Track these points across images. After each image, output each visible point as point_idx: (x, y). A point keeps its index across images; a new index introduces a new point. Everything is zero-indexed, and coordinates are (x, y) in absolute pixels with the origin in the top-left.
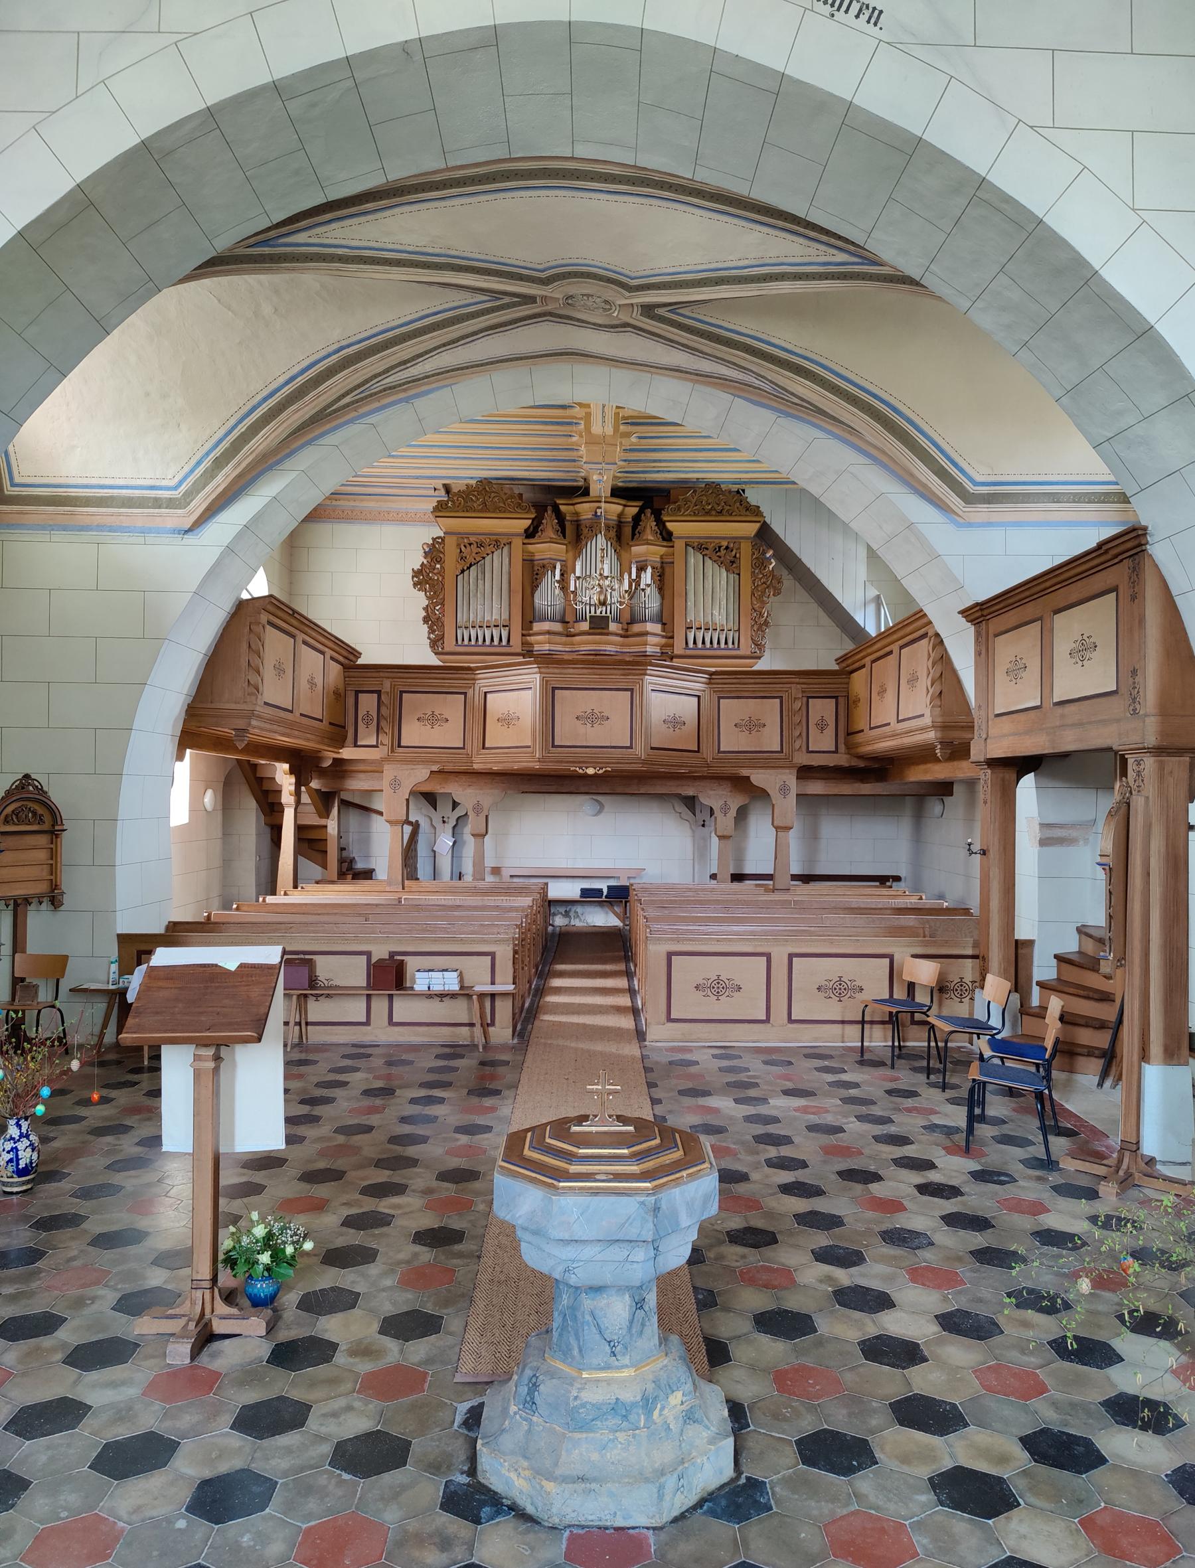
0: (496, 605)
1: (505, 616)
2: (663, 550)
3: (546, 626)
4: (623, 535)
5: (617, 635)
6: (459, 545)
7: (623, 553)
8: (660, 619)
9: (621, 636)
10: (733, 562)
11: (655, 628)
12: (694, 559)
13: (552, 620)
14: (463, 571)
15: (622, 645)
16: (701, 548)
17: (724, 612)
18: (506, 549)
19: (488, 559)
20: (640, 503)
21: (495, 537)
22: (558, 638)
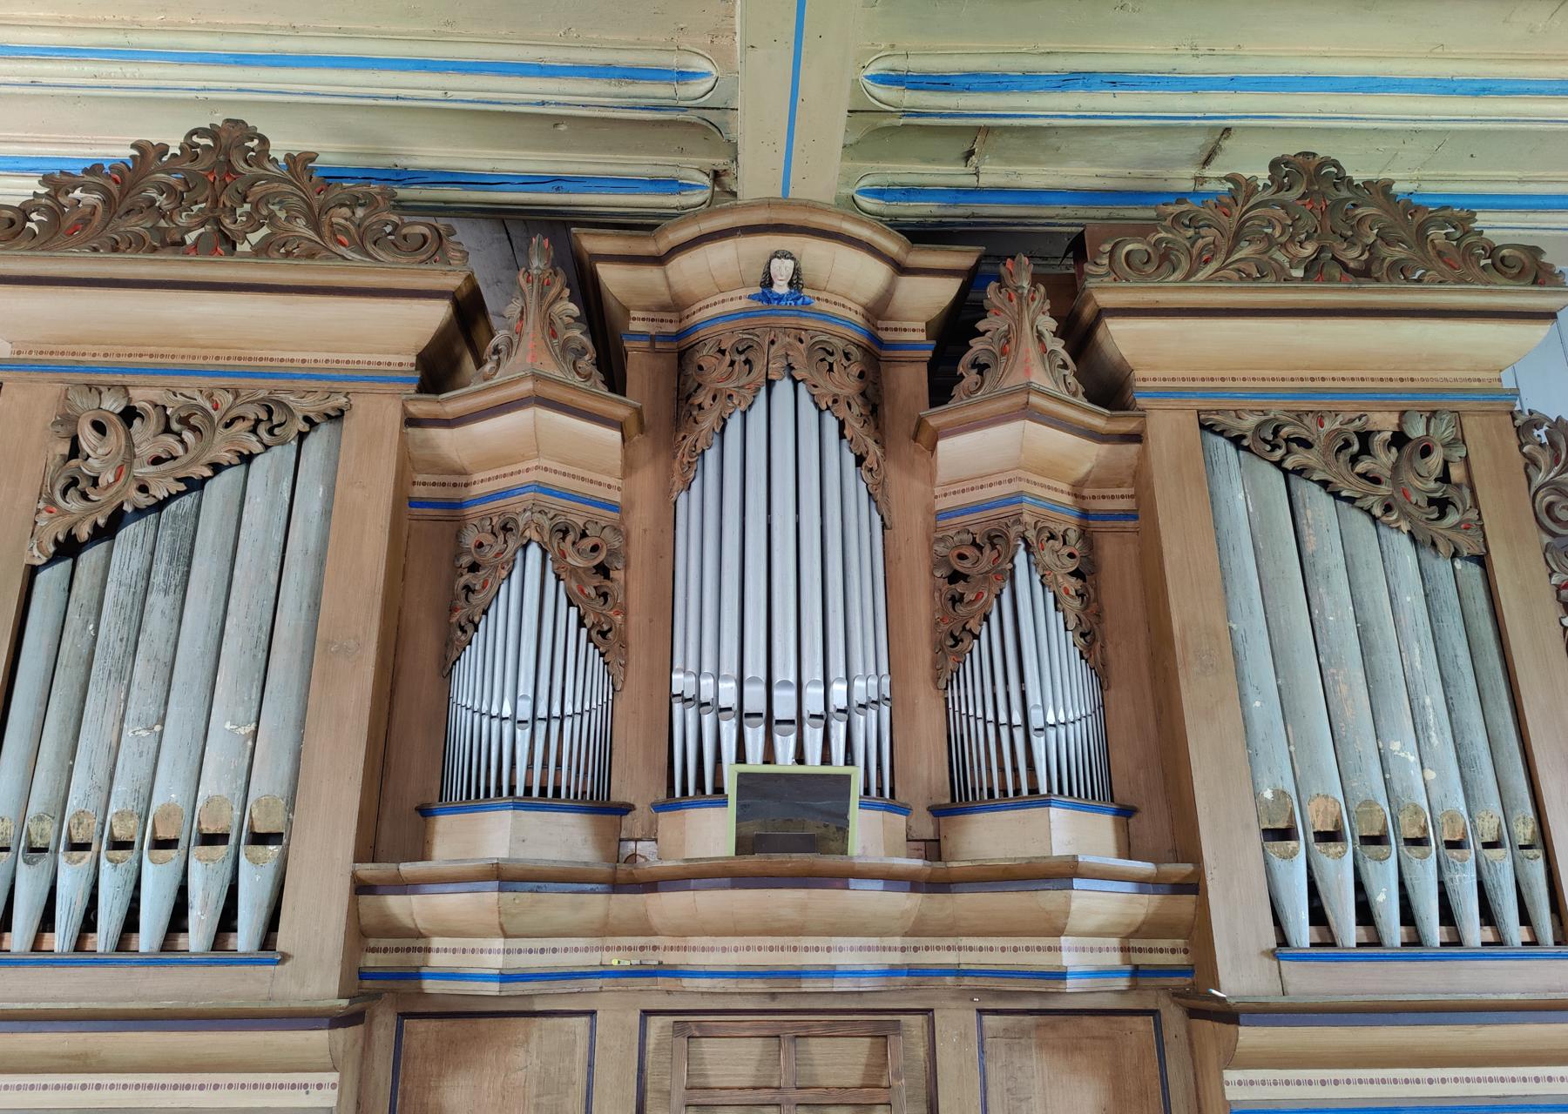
0: (227, 725)
1: (269, 782)
2: (1086, 456)
3: (496, 835)
4: (900, 386)
5: (893, 879)
6: (67, 421)
7: (895, 477)
8: (1100, 788)
9: (915, 883)
10: (1442, 505)
11: (1073, 832)
12: (1246, 490)
13: (543, 798)
14: (68, 549)
15: (918, 929)
16: (1273, 443)
17: (1440, 741)
18: (315, 445)
19: (219, 489)
20: (963, 258)
21: (263, 388)
22: (558, 905)
